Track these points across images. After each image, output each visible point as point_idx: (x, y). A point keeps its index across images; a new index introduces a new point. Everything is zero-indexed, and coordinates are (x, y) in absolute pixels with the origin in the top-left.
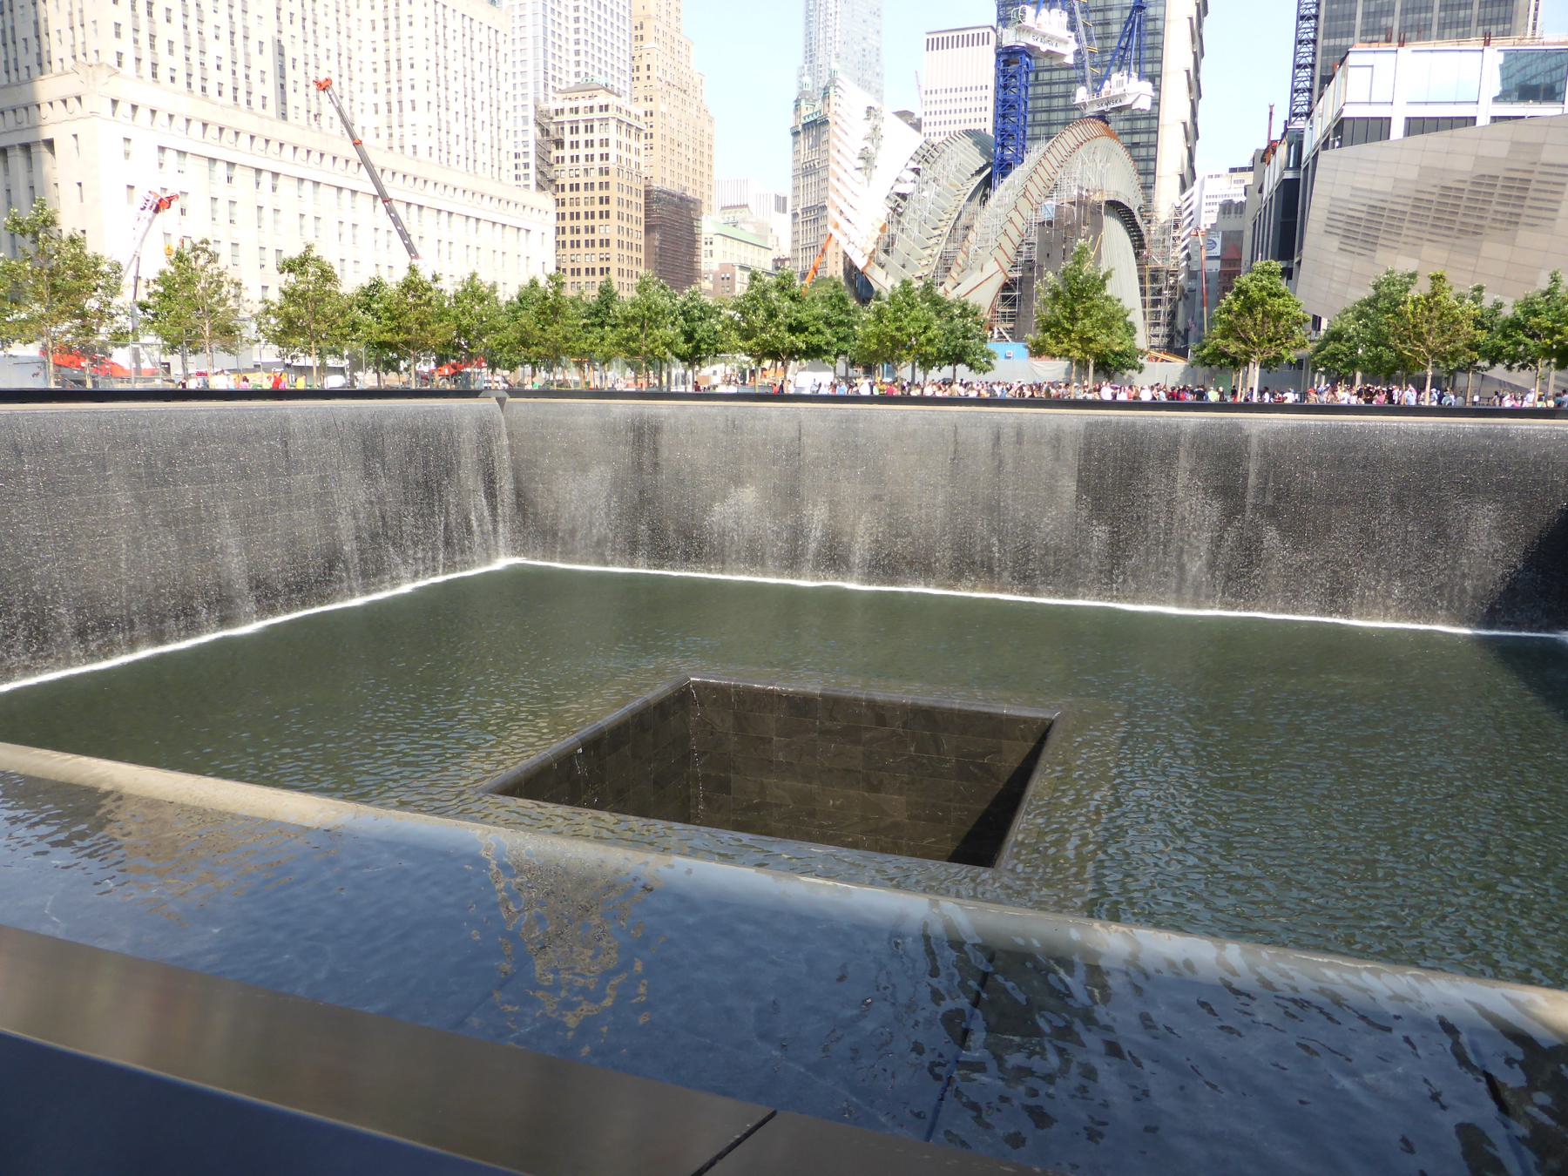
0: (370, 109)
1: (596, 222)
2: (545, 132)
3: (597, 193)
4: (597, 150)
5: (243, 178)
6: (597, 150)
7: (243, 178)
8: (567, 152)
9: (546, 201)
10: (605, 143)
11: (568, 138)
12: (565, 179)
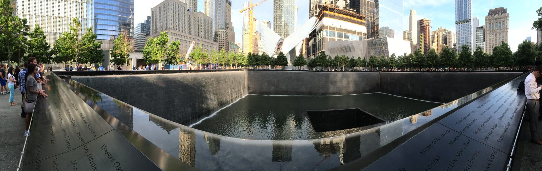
0: (196, 32)
1: (222, 46)
2: (216, 34)
3: (222, 43)
4: (222, 37)
5: (184, 42)
6: (222, 37)
7: (184, 42)
8: (218, 37)
9: (216, 43)
10: (223, 36)
11: (219, 35)
12: (218, 41)
